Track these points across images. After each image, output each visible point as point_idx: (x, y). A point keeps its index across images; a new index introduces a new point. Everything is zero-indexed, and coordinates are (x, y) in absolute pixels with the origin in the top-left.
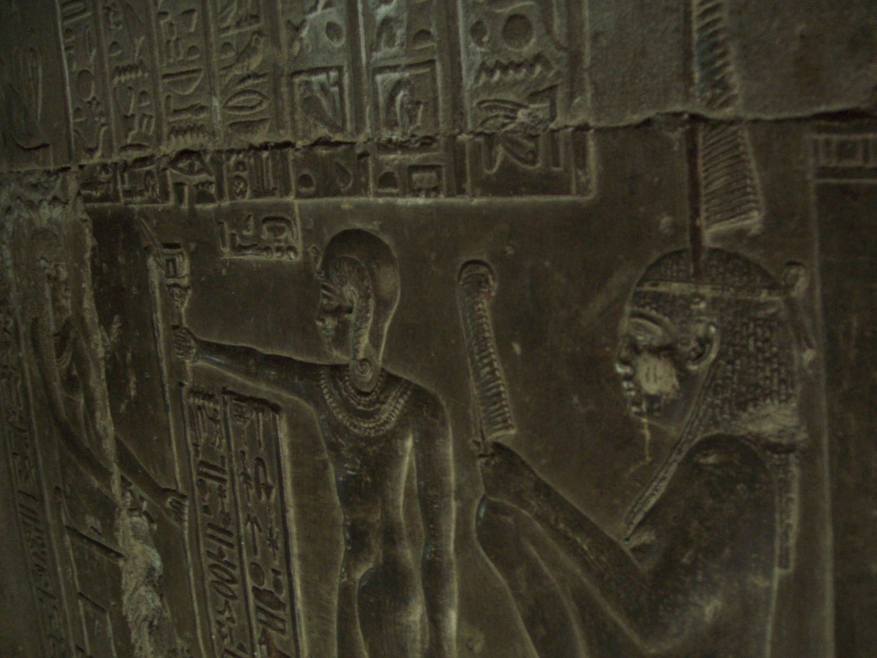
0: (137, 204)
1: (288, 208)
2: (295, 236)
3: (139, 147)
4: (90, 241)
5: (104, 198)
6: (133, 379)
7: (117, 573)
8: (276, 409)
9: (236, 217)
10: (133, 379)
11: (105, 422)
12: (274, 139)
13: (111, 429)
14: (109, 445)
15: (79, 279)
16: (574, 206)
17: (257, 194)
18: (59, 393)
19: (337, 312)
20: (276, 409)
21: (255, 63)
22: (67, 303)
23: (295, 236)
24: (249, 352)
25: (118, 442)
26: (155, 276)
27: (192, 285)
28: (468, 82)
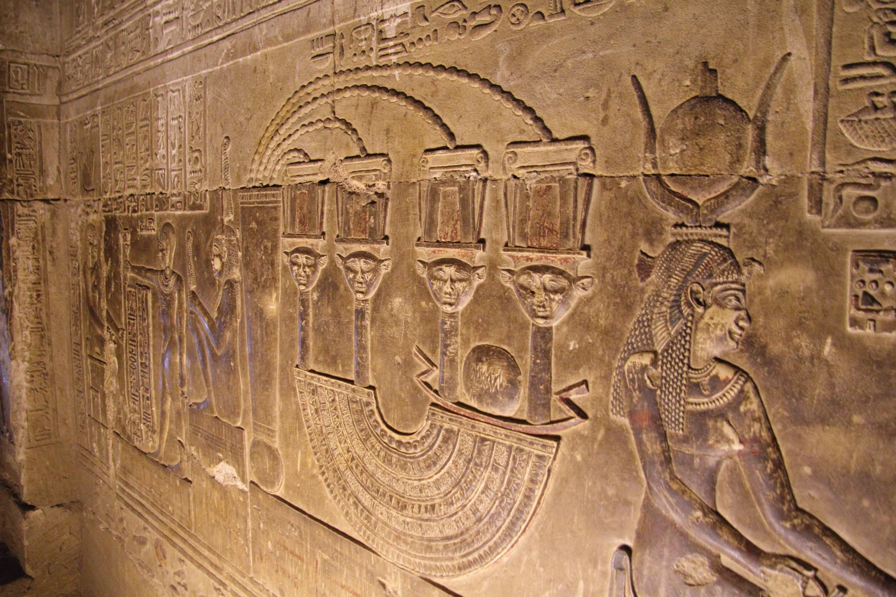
0: (117, 214)
1: (153, 215)
2: (154, 225)
3: (119, 192)
4: (104, 229)
5: (109, 211)
6: (113, 283)
7: (103, 370)
8: (148, 288)
9: (141, 218)
10: (113, 283)
11: (104, 305)
12: (151, 192)
13: (106, 307)
14: (104, 313)
15: (100, 244)
16: (205, 214)
17: (147, 210)
18: (91, 294)
19: (162, 250)
20: (148, 288)
21: (148, 165)
22: (95, 254)
23: (154, 225)
24: (143, 268)
25: (108, 312)
26: (121, 241)
27: (132, 243)
28: (188, 176)
